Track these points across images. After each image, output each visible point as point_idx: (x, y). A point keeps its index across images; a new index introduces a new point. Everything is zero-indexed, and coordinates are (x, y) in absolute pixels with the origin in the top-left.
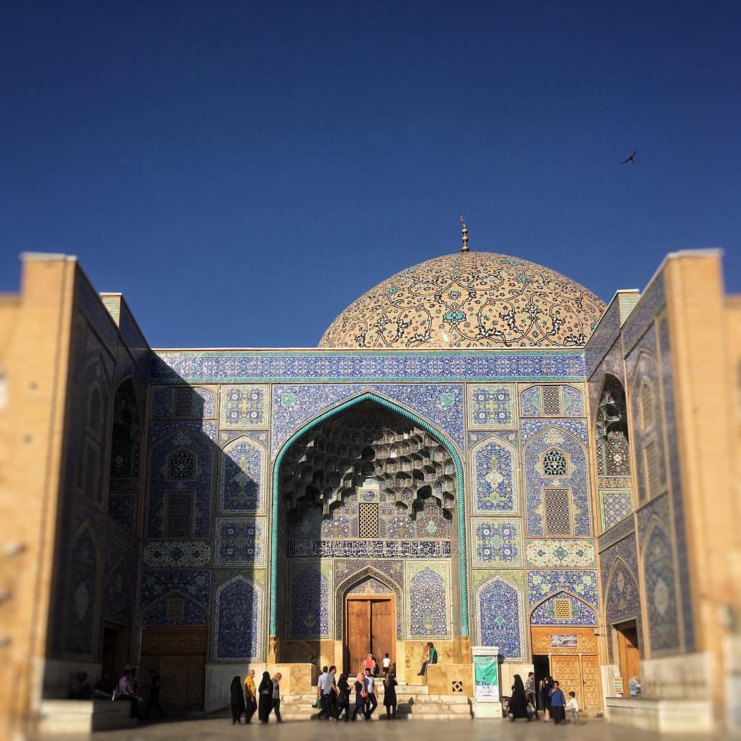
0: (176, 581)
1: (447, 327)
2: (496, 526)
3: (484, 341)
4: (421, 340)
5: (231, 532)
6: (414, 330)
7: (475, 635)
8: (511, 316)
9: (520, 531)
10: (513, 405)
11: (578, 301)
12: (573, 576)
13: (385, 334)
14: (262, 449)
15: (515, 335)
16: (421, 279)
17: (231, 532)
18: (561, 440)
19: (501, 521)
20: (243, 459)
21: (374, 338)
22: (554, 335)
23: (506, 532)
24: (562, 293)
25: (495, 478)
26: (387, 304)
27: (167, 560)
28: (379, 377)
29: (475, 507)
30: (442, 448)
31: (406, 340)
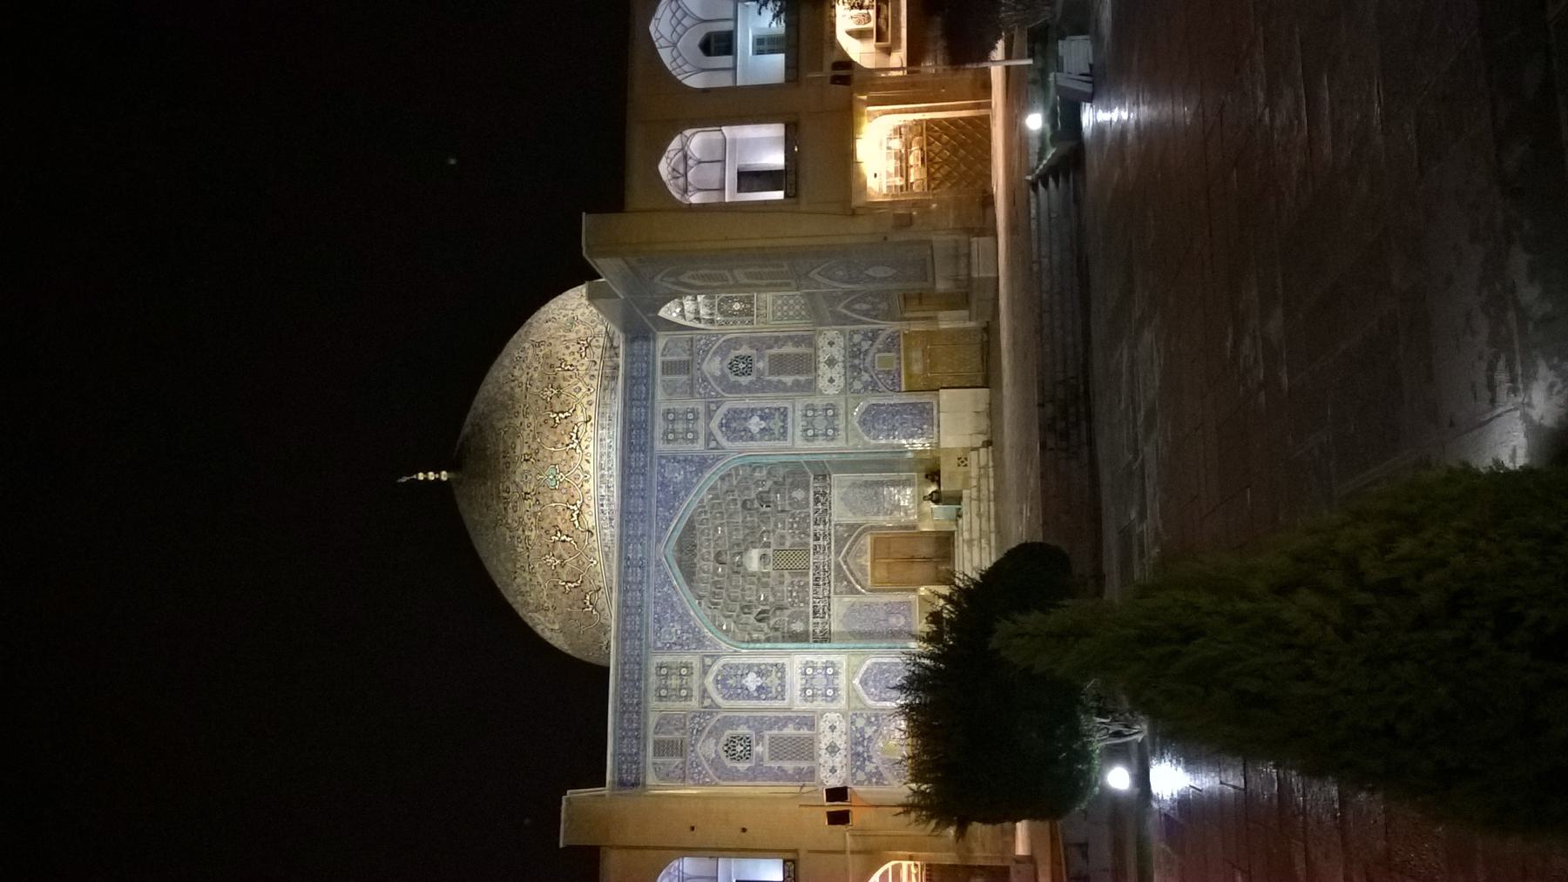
0: (860, 749)
3: (584, 444)
5: (809, 692)
10: (678, 405)
11: (537, 345)
12: (854, 353)
14: (722, 661)
17: (809, 692)
23: (810, 413)
25: (755, 424)
27: (839, 759)
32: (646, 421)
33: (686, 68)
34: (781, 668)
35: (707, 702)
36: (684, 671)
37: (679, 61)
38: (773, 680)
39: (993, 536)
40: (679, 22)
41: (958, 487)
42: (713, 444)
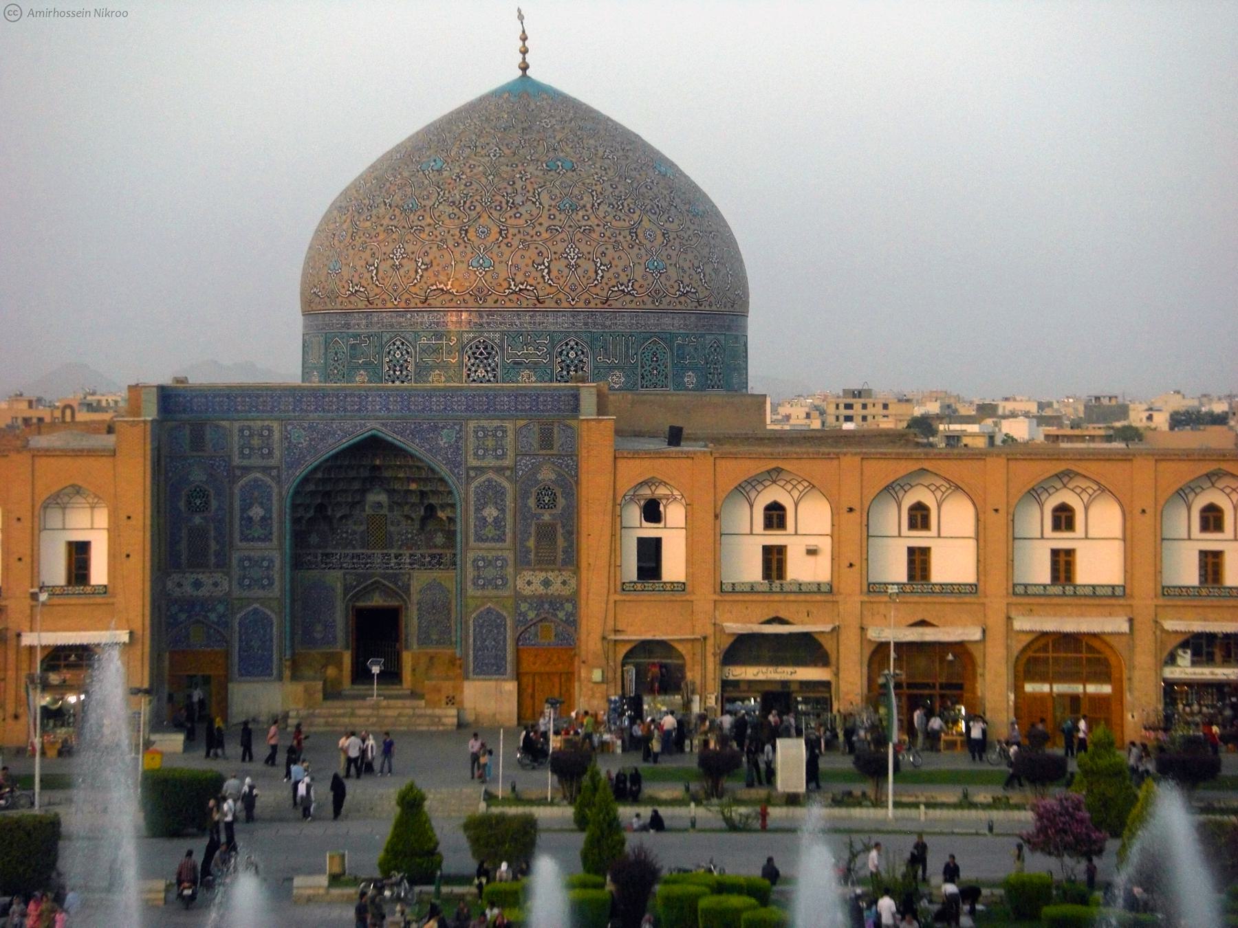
0: (198, 609)
3: (514, 297)
5: (246, 564)
7: (467, 655)
9: (511, 562)
11: (633, 231)
12: (555, 603)
13: (402, 271)
14: (273, 485)
15: (549, 289)
17: (246, 564)
18: (553, 477)
19: (494, 553)
23: (499, 563)
24: (614, 223)
25: (491, 512)
27: (188, 589)
29: (472, 538)
30: (442, 480)
32: (495, 410)
34: (267, 538)
37: (760, 488)
38: (258, 531)
40: (794, 486)
41: (427, 697)
42: (472, 474)
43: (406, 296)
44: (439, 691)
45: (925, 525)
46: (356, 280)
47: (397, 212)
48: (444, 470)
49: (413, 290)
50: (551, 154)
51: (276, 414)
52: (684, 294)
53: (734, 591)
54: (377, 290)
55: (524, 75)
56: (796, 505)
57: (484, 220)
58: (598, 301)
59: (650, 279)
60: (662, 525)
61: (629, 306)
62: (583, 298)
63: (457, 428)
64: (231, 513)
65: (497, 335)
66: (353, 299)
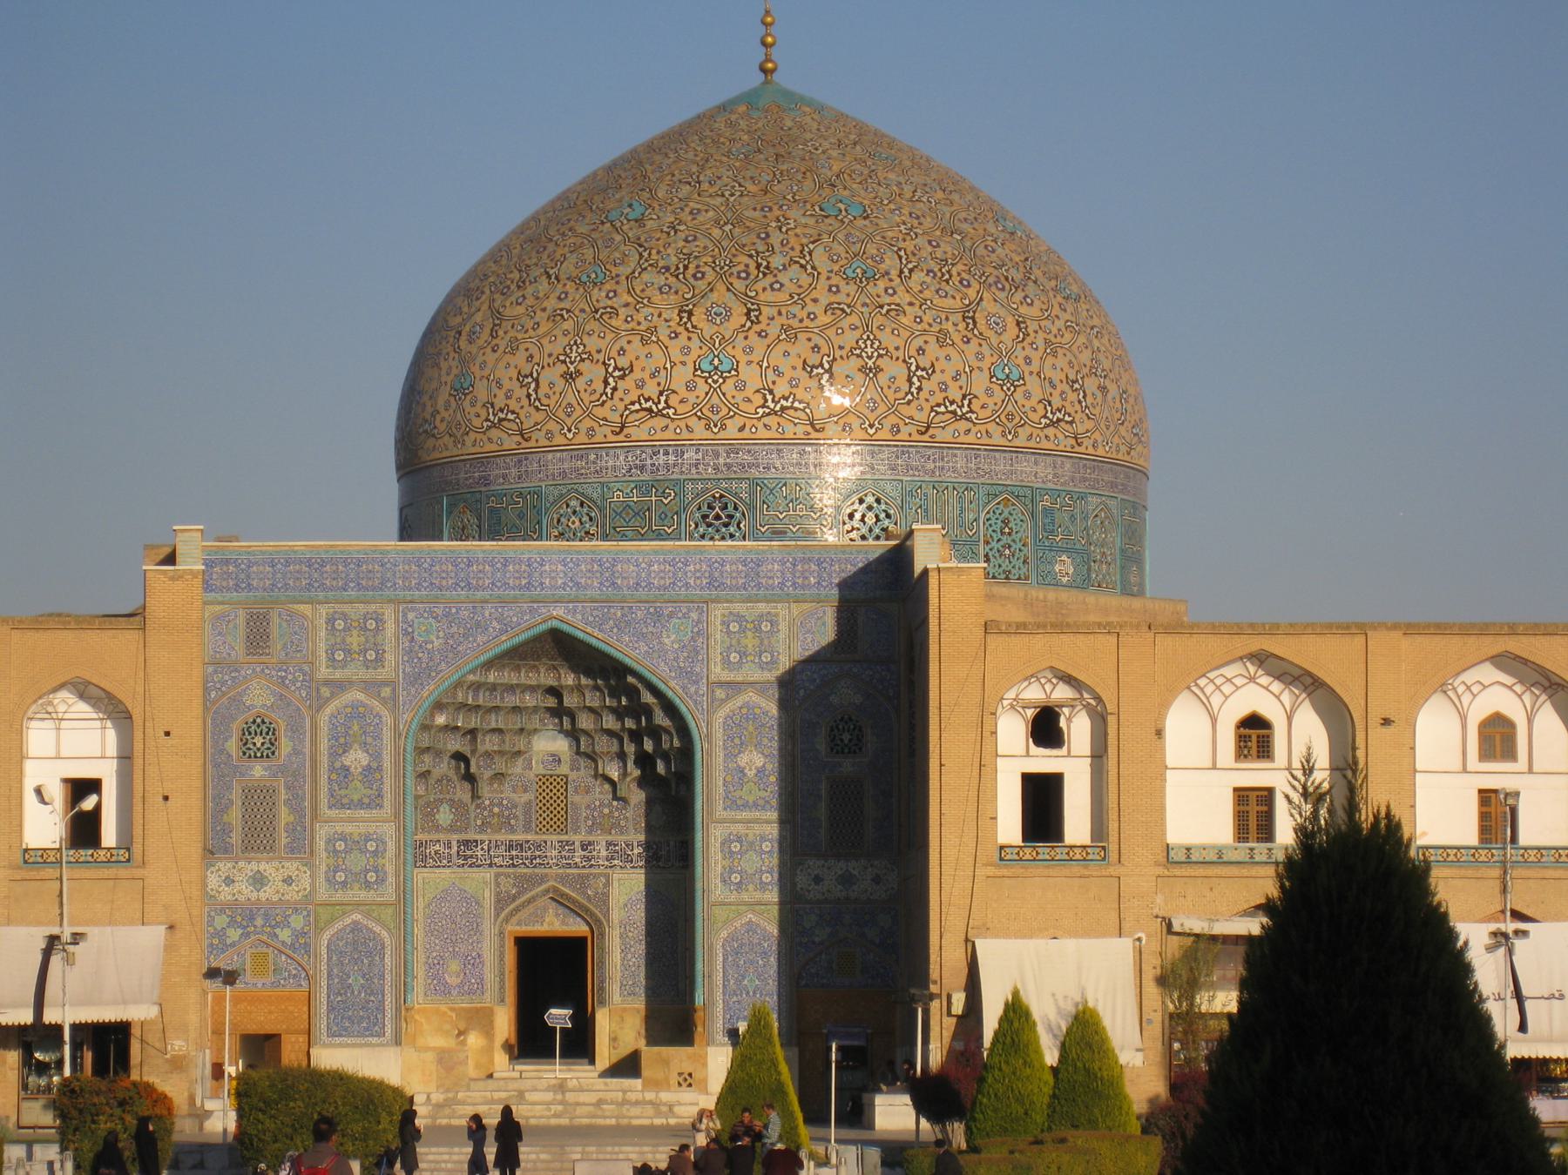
0: (259, 922)
1: (702, 387)
2: (751, 838)
4: (650, 410)
5: (340, 846)
6: (638, 387)
8: (827, 366)
13: (581, 383)
16: (655, 256)
17: (340, 846)
18: (858, 699)
20: (356, 728)
21: (558, 389)
22: (909, 403)
26: (583, 311)
27: (244, 890)
28: (571, 592)
29: (719, 805)
31: (621, 406)
32: (759, 586)
33: (1216, 700)
34: (375, 802)
35: (326, 692)
36: (371, 655)
37: (1227, 689)
38: (358, 790)
39: (564, 1121)
41: (645, 1072)
43: (588, 423)
44: (666, 1063)
45: (1509, 753)
46: (499, 403)
47: (570, 287)
48: (674, 689)
49: (600, 412)
50: (827, 191)
51: (388, 593)
52: (1053, 424)
53: (1189, 862)
54: (540, 416)
55: (766, 82)
56: (1290, 719)
57: (720, 295)
58: (913, 429)
59: (999, 395)
60: (1064, 751)
61: (963, 439)
62: (887, 424)
63: (694, 615)
64: (314, 761)
65: (744, 485)
66: (494, 433)
